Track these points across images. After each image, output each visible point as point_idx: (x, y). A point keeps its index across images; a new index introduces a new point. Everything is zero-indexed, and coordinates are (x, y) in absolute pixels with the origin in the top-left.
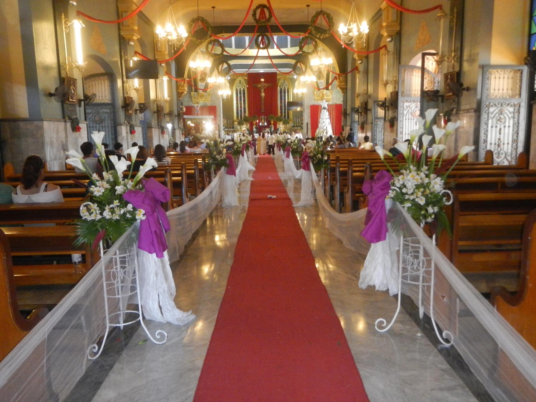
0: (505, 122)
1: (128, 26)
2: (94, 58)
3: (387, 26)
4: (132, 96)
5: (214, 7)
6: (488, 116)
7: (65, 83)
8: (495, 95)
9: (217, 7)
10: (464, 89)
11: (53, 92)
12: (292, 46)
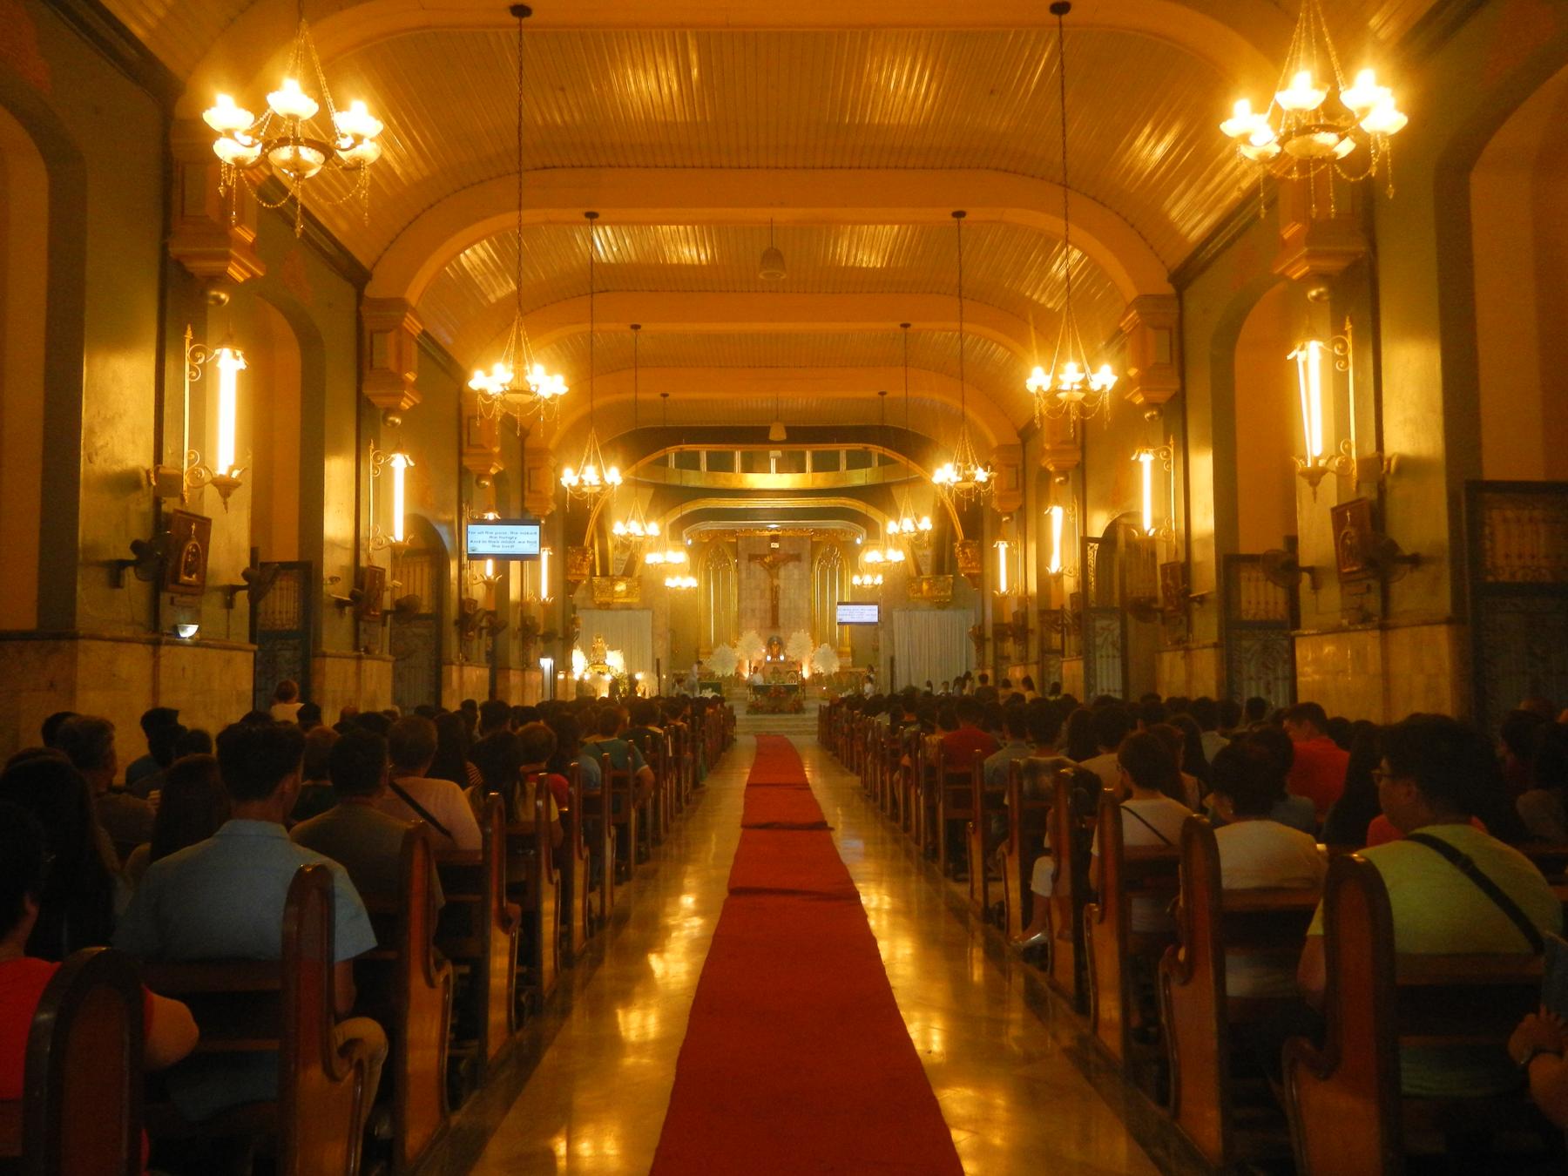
1: (482, 446)
2: (421, 525)
3: (1054, 452)
4: (475, 597)
5: (665, 395)
7: (364, 580)
9: (673, 396)
12: (849, 467)
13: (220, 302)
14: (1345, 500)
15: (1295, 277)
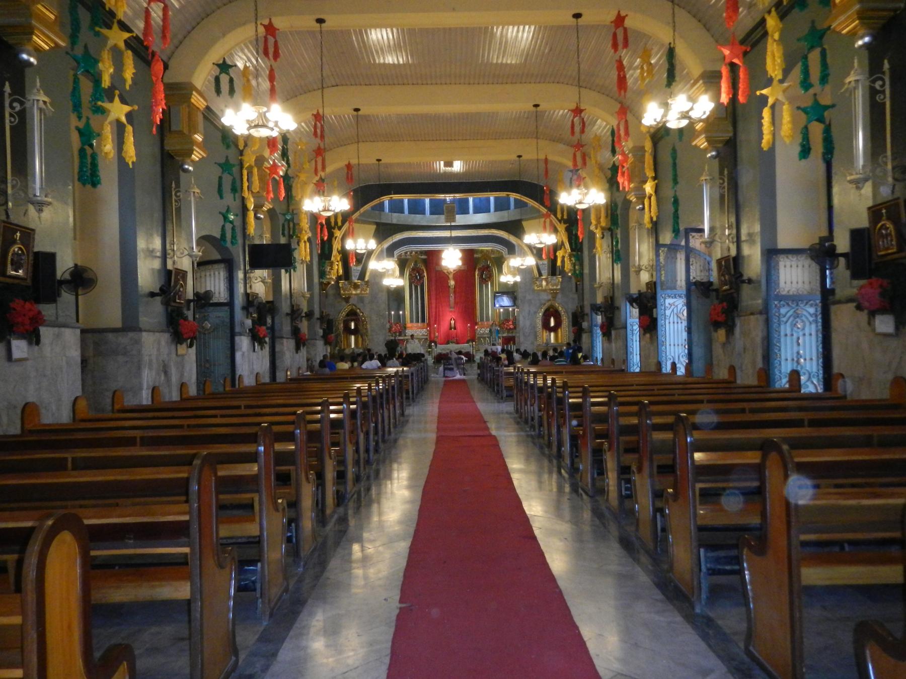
0: (803, 329)
6: (779, 320)
8: (787, 290)
10: (743, 282)
11: (158, 291)
13: (28, 64)
14: (879, 201)
15: (844, 32)
